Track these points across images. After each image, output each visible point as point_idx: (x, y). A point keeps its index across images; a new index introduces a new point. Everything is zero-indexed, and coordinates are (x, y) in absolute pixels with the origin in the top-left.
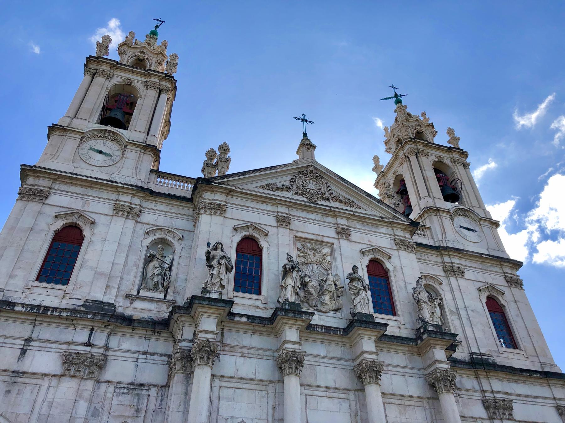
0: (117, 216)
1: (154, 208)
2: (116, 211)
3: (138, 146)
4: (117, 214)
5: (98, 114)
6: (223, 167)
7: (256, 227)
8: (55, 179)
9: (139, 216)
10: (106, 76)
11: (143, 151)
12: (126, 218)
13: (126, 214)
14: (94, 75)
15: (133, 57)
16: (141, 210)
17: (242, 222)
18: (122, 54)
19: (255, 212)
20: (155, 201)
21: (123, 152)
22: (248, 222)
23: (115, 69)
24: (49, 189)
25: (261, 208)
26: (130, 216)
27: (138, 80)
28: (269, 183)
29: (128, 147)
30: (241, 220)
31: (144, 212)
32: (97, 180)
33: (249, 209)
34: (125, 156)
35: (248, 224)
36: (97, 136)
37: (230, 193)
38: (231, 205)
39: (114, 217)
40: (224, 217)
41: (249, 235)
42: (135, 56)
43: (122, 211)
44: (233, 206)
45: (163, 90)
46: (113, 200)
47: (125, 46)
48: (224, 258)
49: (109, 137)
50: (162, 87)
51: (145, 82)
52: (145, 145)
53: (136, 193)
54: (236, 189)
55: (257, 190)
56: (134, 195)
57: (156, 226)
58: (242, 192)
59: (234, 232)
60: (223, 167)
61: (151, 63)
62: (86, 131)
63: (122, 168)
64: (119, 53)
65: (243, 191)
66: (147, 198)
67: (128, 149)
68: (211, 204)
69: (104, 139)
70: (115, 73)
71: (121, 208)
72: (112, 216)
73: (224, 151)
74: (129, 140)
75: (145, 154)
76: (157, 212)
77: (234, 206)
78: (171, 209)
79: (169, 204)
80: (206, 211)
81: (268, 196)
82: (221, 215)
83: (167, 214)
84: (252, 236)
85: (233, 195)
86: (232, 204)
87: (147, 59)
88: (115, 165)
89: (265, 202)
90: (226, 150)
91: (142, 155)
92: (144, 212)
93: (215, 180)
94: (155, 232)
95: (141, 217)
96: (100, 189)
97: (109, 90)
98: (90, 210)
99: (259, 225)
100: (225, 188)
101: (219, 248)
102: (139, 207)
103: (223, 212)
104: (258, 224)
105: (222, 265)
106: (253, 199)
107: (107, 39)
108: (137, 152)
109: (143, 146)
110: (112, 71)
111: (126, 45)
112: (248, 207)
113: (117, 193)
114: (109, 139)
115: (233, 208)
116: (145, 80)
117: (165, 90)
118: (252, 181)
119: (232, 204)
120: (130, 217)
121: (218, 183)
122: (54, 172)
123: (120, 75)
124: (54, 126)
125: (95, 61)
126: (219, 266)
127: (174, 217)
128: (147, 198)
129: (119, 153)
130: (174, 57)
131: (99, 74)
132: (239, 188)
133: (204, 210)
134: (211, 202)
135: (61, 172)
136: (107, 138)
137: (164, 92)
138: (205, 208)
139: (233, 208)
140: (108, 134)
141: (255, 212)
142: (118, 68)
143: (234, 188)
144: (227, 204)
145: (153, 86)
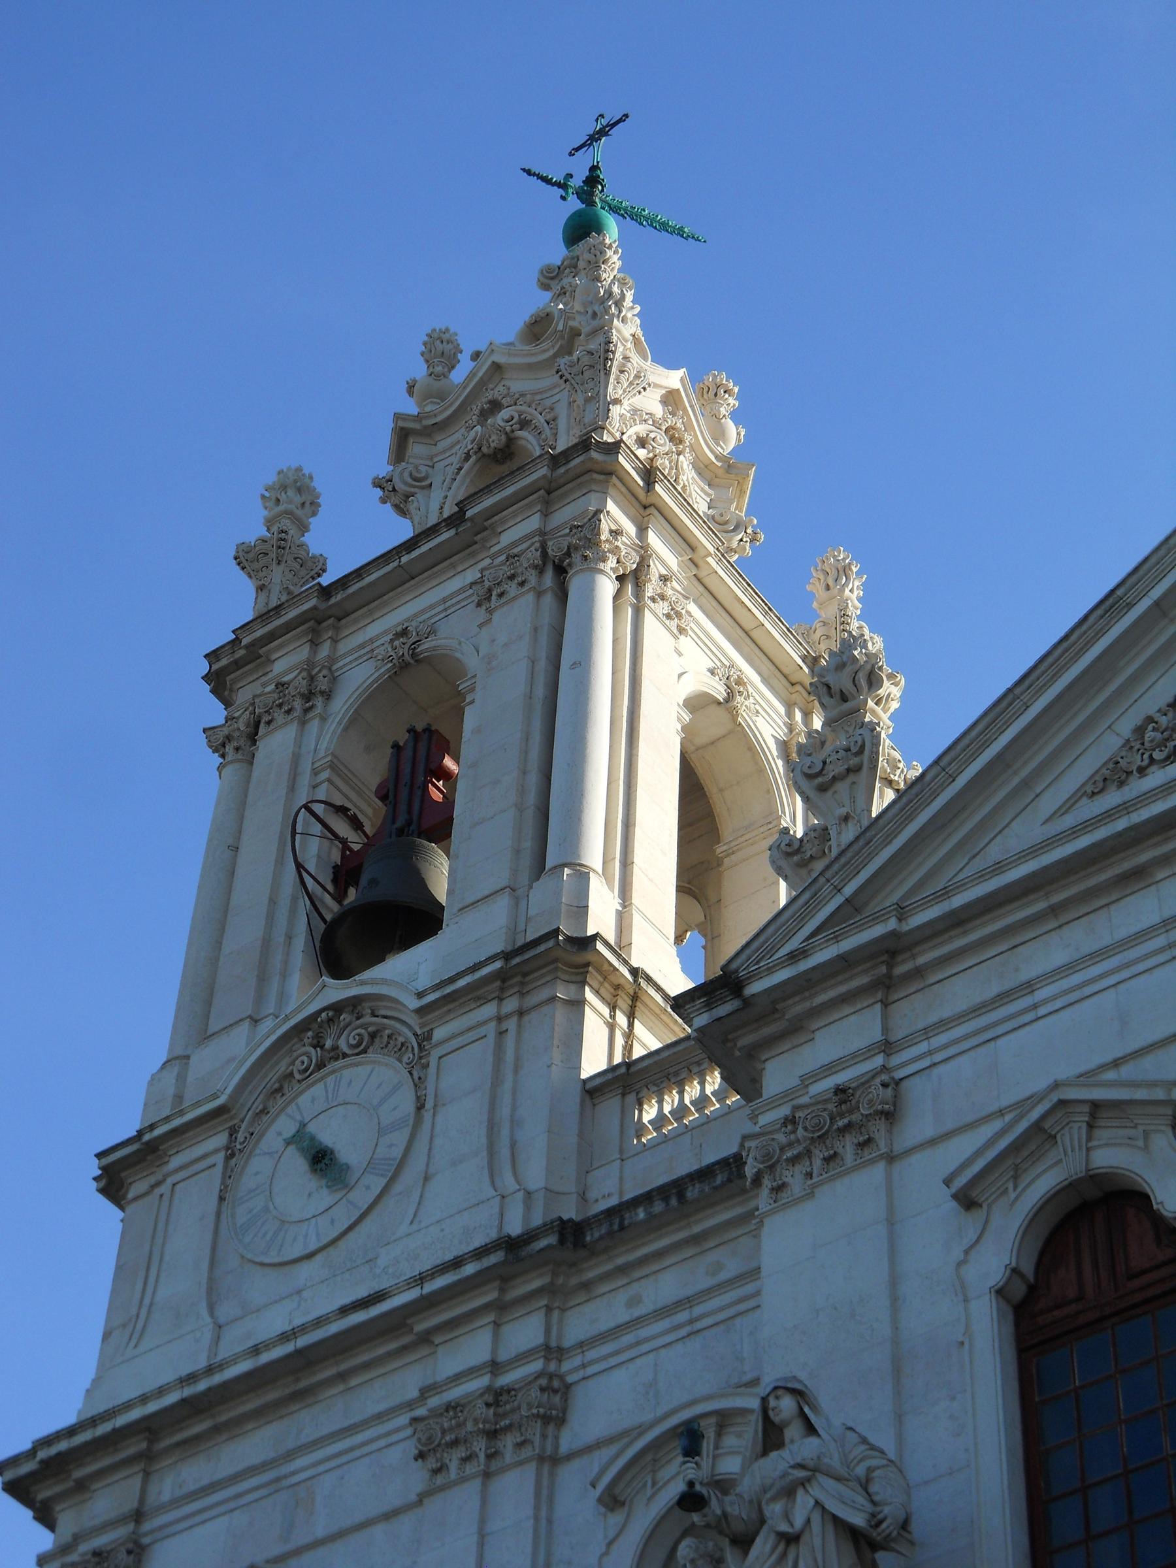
0: (442, 1488)
1: (623, 1316)
2: (432, 1463)
3: (473, 995)
4: (440, 1480)
5: (300, 940)
6: (846, 819)
7: (1096, 1107)
8: (147, 1458)
9: (555, 1419)
10: (298, 704)
11: (511, 1004)
12: (487, 1475)
13: (480, 1446)
14: (253, 738)
15: (460, 469)
16: (551, 1377)
17: (1008, 1118)
18: (407, 496)
19: (1088, 990)
20: (623, 1270)
21: (419, 1083)
22: (1023, 1105)
23: (337, 629)
24: (131, 1527)
25: (1122, 933)
26: (508, 1442)
27: (444, 600)
28: (1138, 721)
29: (439, 1034)
30: (1001, 1113)
31: (581, 1374)
32: (302, 1341)
33: (1042, 994)
34: (429, 1104)
35: (1035, 1114)
36: (291, 1074)
37: (900, 970)
38: (923, 1047)
39: (433, 1505)
40: (891, 1158)
41: (1071, 1187)
42: (467, 457)
43: (455, 1443)
44: (937, 1041)
45: (568, 554)
46: (410, 1405)
47: (416, 449)
48: (803, 1483)
49: (343, 1045)
50: (555, 549)
51: (472, 584)
52: (498, 965)
53: (502, 1290)
54: (918, 919)
55: (1068, 821)
56: (501, 1307)
57: (642, 1429)
58: (953, 913)
59: (971, 1223)
60: (846, 819)
61: (547, 432)
62: (228, 1091)
63: (427, 1179)
64: (397, 507)
65: (958, 901)
66: (574, 1281)
67: (441, 1043)
68: (790, 1121)
69: (329, 1068)
70: (343, 647)
71: (451, 1429)
72: (420, 1502)
73: (844, 698)
74: (420, 995)
75: (526, 1018)
76: (644, 1333)
77: (942, 1039)
78: (718, 1267)
79: (696, 1240)
80: (779, 1189)
81: (1121, 824)
82: (867, 1154)
83: (698, 1310)
84: (1094, 1178)
85: (918, 973)
86: (928, 1032)
87: (524, 424)
88: (398, 1187)
89: (1137, 877)
90: (848, 686)
91: (510, 1040)
92: (581, 1374)
93: (774, 949)
94: (654, 1472)
95: (576, 1417)
96: (342, 1377)
97: (332, 766)
98: (320, 1533)
99: (1126, 1071)
100: (845, 963)
101: (786, 1424)
102: (537, 1365)
103: (878, 1130)
104: (1116, 1063)
105: (805, 1538)
106: (1054, 910)
107: (283, 497)
108: (482, 1031)
109: (502, 977)
110: (324, 651)
111: (411, 440)
112: (1028, 987)
113: (425, 1350)
114: (345, 1056)
115: (938, 1057)
116: (471, 575)
117: (577, 548)
118: (1026, 784)
119: (928, 1032)
120: (509, 1456)
121: (794, 957)
122: (121, 1421)
123: (362, 646)
124: (107, 1160)
125: (237, 665)
126: (784, 1555)
127: (742, 1307)
128: (574, 1281)
129: (405, 1101)
130: (595, 314)
131: (266, 718)
132: (927, 903)
133: (767, 1183)
134: (785, 1111)
135: (144, 1399)
136: (337, 1054)
137: (576, 557)
138: (772, 1167)
139: (938, 1057)
140: (334, 1029)
141: (1088, 990)
142: (341, 616)
143: (892, 924)
144: (896, 1060)
145: (512, 578)
